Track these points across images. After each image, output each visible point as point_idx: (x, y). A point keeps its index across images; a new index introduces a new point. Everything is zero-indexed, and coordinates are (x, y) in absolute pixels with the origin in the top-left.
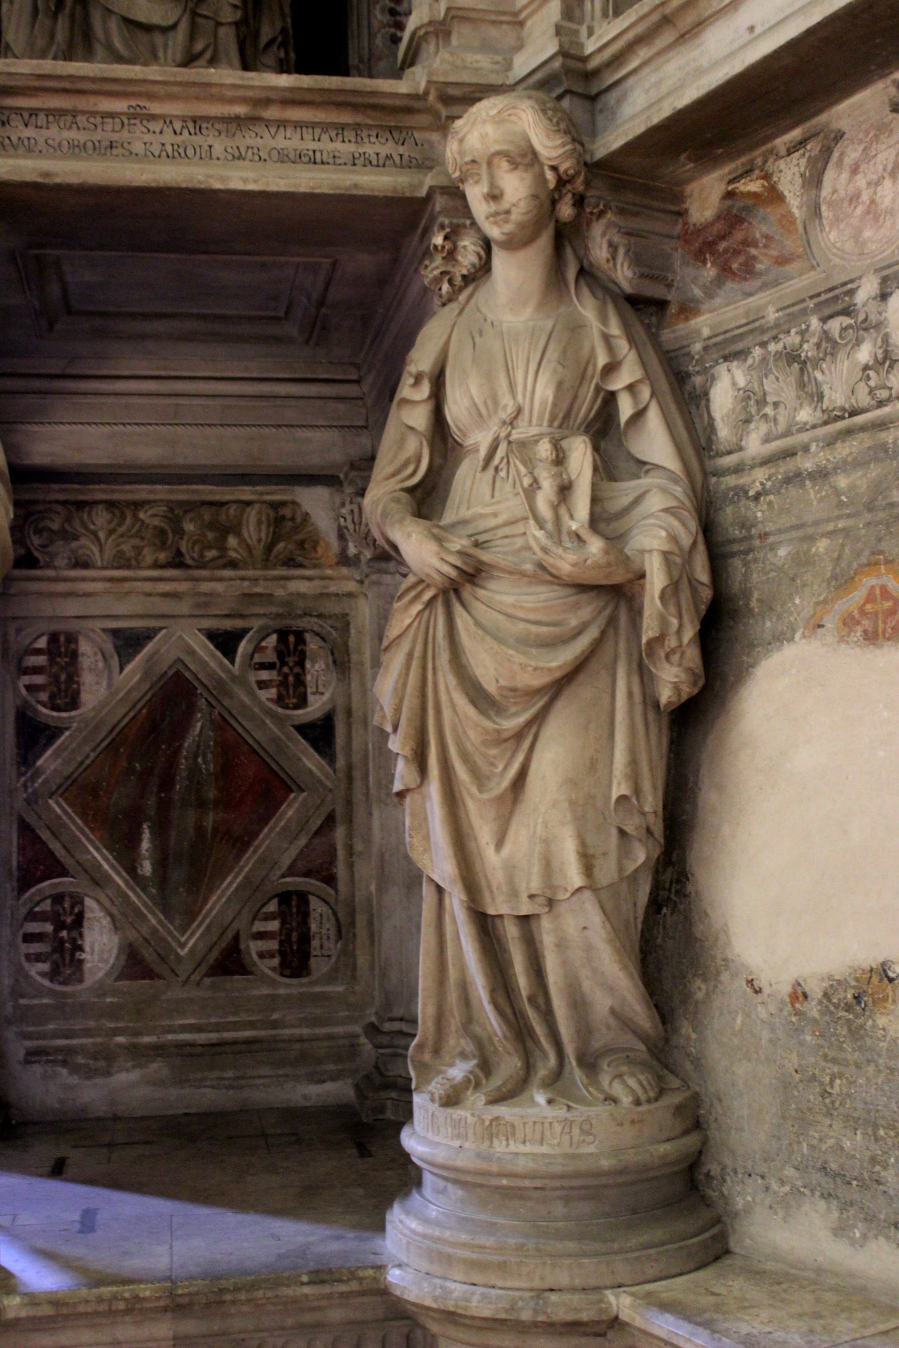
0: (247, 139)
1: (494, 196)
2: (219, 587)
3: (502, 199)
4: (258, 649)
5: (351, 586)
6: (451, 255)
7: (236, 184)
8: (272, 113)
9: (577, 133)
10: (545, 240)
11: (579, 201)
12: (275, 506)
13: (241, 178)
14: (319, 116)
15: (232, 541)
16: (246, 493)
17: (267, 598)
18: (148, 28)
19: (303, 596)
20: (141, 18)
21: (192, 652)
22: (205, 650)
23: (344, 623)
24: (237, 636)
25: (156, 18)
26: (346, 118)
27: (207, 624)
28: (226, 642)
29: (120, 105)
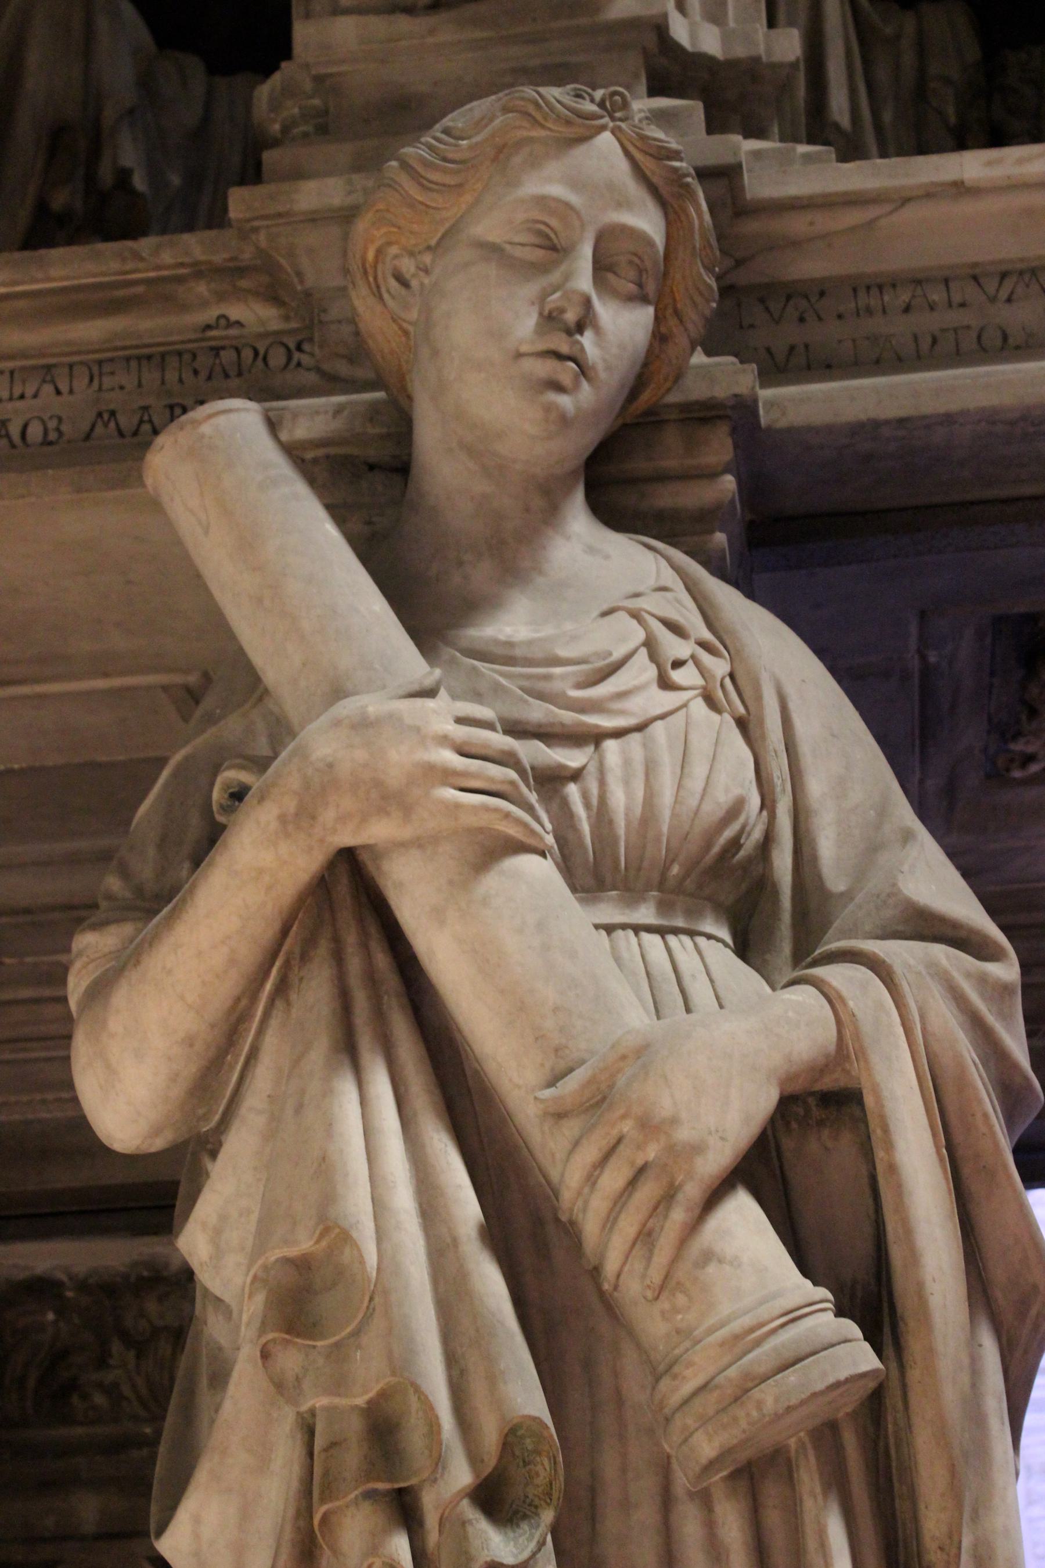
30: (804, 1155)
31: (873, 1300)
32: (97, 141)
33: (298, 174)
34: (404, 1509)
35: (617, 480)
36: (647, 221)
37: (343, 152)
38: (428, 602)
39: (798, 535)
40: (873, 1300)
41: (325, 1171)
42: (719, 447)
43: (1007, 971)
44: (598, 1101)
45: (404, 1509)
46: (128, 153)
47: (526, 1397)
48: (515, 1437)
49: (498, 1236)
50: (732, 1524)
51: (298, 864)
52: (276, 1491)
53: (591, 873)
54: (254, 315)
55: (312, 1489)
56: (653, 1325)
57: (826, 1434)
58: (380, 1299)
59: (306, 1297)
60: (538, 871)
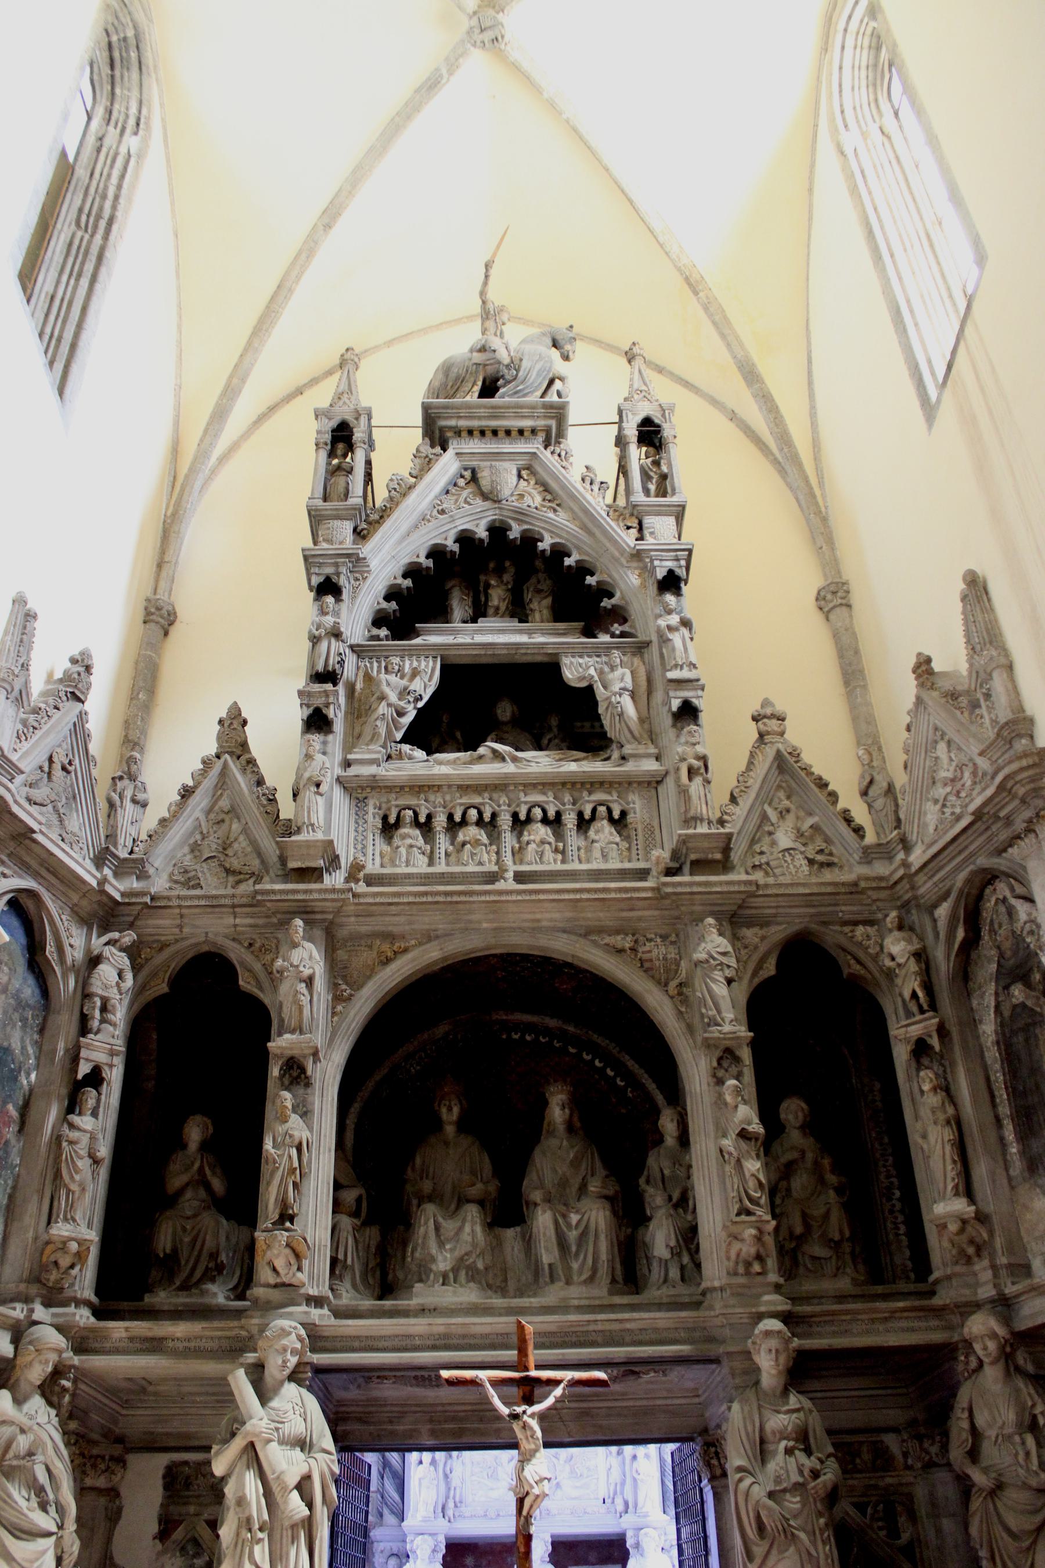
0: (890, 1325)
1: (985, 1349)
2: (855, 1482)
3: (987, 1349)
4: (876, 1511)
5: (912, 1480)
6: (967, 1363)
7: (891, 1344)
8: (898, 1315)
9: (1006, 1320)
10: (1002, 1361)
11: (1012, 1345)
12: (875, 1443)
13: (893, 1340)
14: (913, 1314)
15: (858, 1461)
16: (861, 1438)
17: (875, 1487)
18: (819, 1258)
19: (891, 1485)
20: (817, 1254)
21: (848, 1514)
22: (852, 1511)
23: (910, 1497)
24: (867, 1504)
25: (823, 1255)
26: (921, 1314)
27: (855, 1500)
28: (861, 1507)
29: (848, 1317)
30: (303, 1486)
31: (310, 1505)
32: (218, 1253)
33: (252, 1317)
34: (250, 1530)
35: (293, 1377)
36: (298, 1346)
37: (259, 1313)
38: (264, 1398)
39: (319, 1379)
40: (310, 1505)
41: (243, 1485)
42: (308, 1368)
43: (335, 1457)
44: (278, 1478)
45: (250, 1530)
46: (223, 1257)
47: (266, 1517)
48: (265, 1522)
49: (265, 1495)
50: (290, 1533)
51: (245, 1443)
52: (234, 1526)
53: (281, 1442)
54: (244, 1333)
55: (239, 1527)
56: (282, 1507)
57: (303, 1521)
58: (249, 1504)
59: (241, 1501)
60: (274, 1444)
